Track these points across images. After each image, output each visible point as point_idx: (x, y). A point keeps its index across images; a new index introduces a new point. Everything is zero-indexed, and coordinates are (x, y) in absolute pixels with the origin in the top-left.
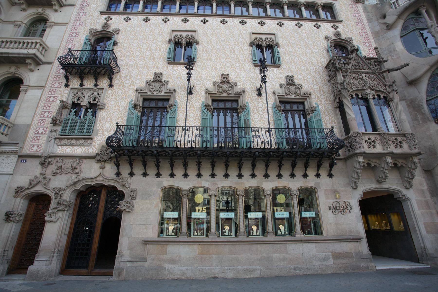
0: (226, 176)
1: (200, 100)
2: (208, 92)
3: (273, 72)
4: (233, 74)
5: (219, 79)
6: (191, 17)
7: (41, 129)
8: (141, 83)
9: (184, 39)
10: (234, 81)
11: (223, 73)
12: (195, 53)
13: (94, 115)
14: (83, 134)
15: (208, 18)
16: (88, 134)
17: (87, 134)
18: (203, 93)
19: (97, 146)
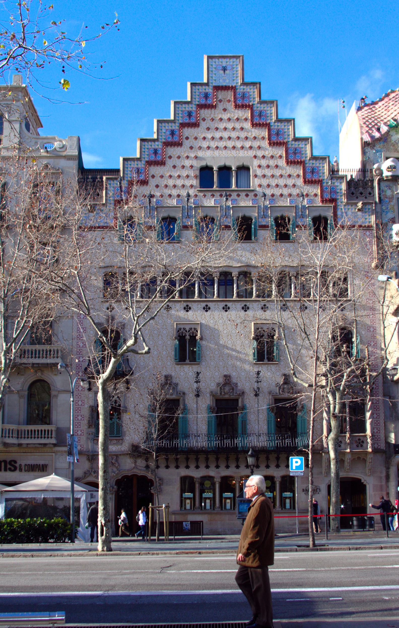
0: (227, 467)
1: (205, 402)
2: (212, 394)
3: (271, 370)
4: (234, 374)
5: (221, 380)
6: (193, 304)
7: (79, 431)
8: (154, 385)
9: (187, 334)
10: (235, 382)
11: (225, 373)
12: (200, 352)
13: (119, 418)
14: (115, 435)
15: (210, 304)
16: (118, 435)
17: (117, 435)
18: (208, 395)
19: (127, 445)
